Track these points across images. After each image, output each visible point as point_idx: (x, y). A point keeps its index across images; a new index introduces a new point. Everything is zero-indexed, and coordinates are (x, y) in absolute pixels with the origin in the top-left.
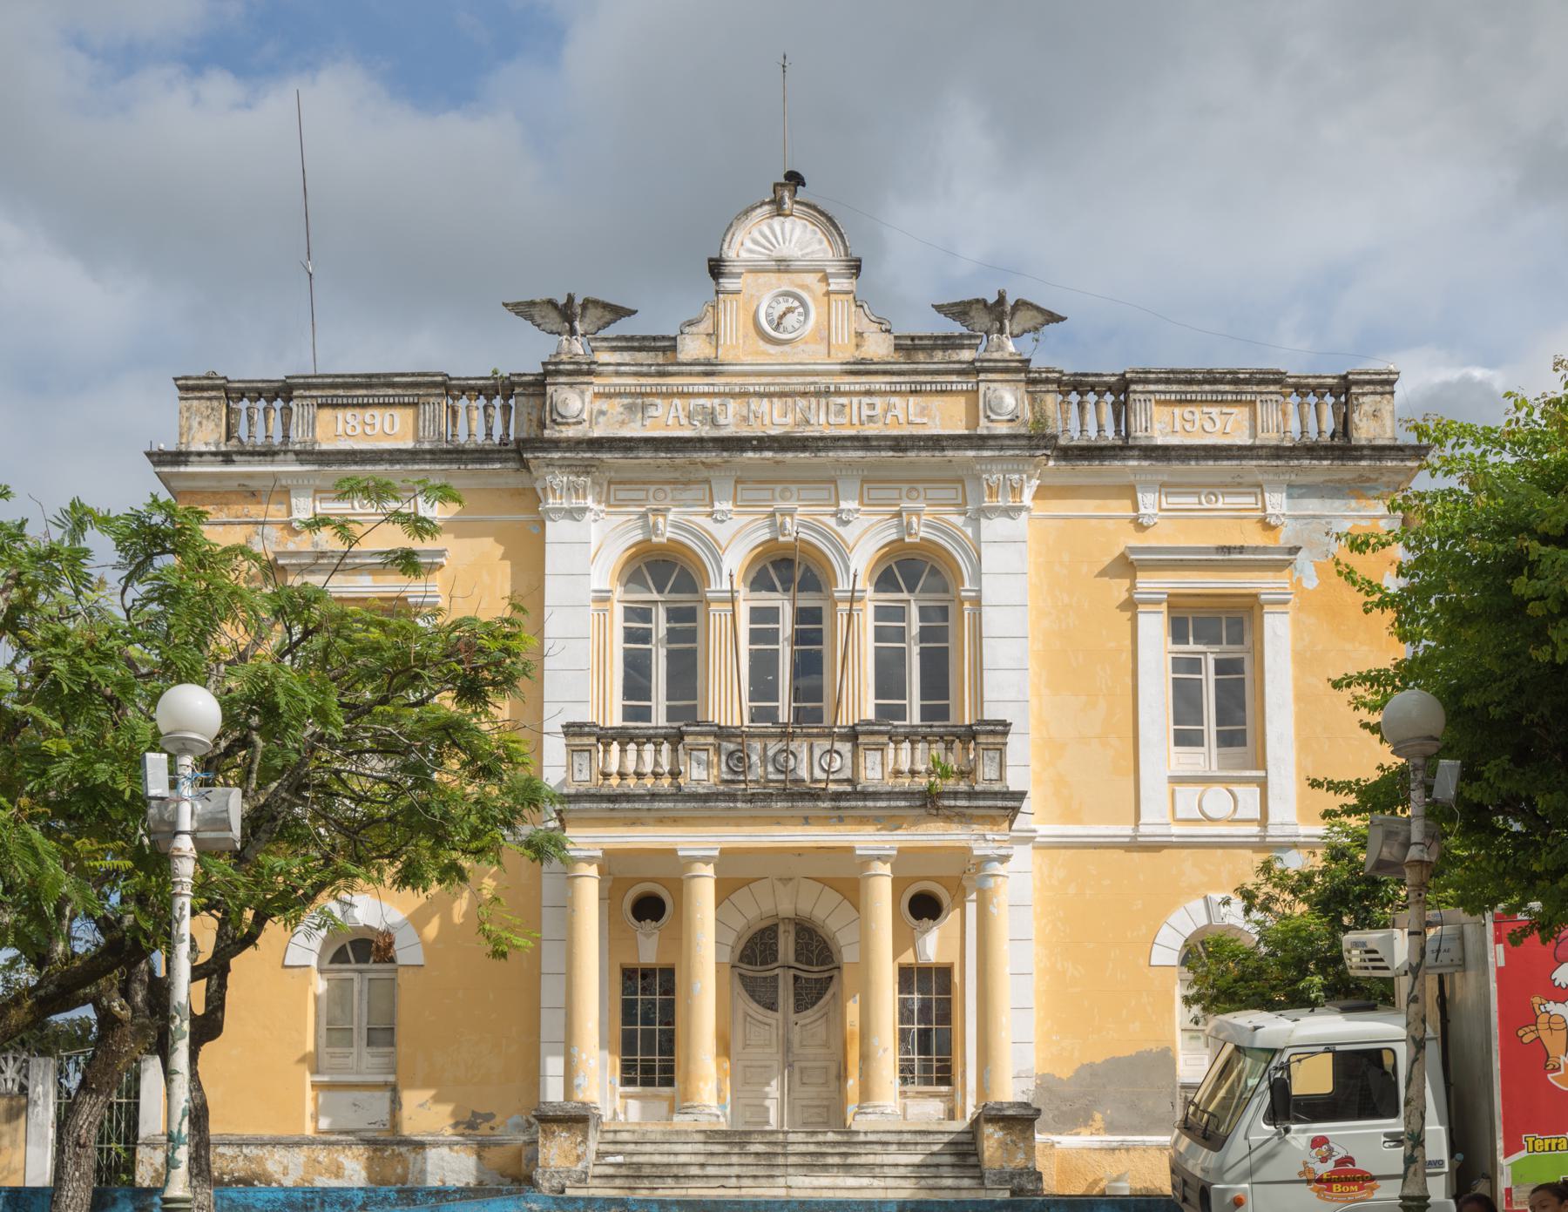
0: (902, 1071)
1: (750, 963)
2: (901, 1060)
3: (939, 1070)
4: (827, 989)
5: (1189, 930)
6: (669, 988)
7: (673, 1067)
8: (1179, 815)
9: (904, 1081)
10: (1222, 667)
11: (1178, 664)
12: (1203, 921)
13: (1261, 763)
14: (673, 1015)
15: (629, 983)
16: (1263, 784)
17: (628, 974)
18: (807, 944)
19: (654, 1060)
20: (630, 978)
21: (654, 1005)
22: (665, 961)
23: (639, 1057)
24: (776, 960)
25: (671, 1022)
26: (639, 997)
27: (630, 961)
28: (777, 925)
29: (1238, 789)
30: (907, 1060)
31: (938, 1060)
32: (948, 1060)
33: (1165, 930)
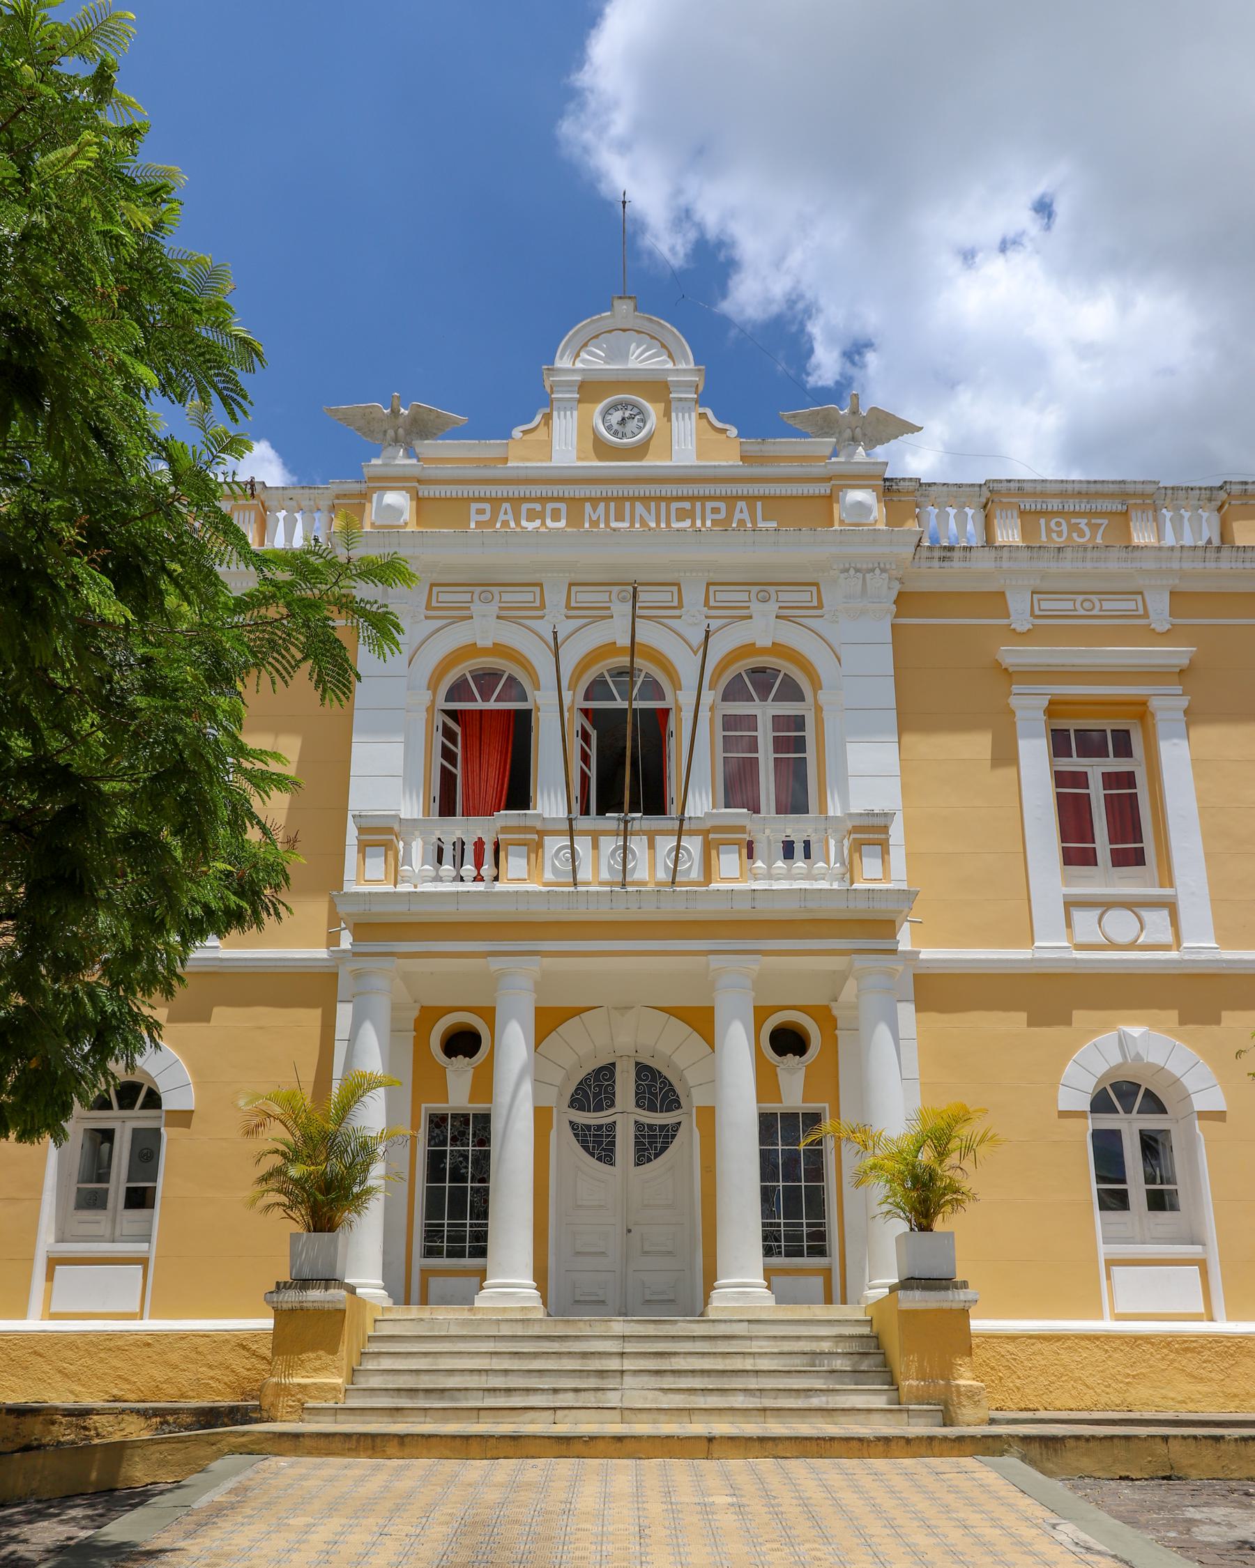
0: (765, 1239)
1: (582, 1108)
2: (764, 1225)
3: (811, 1236)
4: (674, 1136)
5: (1101, 1068)
6: (484, 1140)
7: (486, 1232)
8: (1080, 939)
9: (768, 1252)
10: (1111, 780)
11: (1061, 778)
12: (1116, 1058)
13: (1167, 877)
14: (488, 1171)
15: (437, 1131)
16: (1171, 907)
17: (437, 1121)
18: (650, 1086)
19: (464, 1225)
20: (438, 1126)
21: (466, 1158)
22: (479, 1107)
23: (446, 1222)
24: (612, 1105)
25: (485, 1180)
26: (449, 1148)
27: (439, 1107)
28: (613, 1064)
29: (1147, 915)
30: (771, 1225)
31: (808, 1225)
32: (821, 1225)
33: (1070, 1068)
